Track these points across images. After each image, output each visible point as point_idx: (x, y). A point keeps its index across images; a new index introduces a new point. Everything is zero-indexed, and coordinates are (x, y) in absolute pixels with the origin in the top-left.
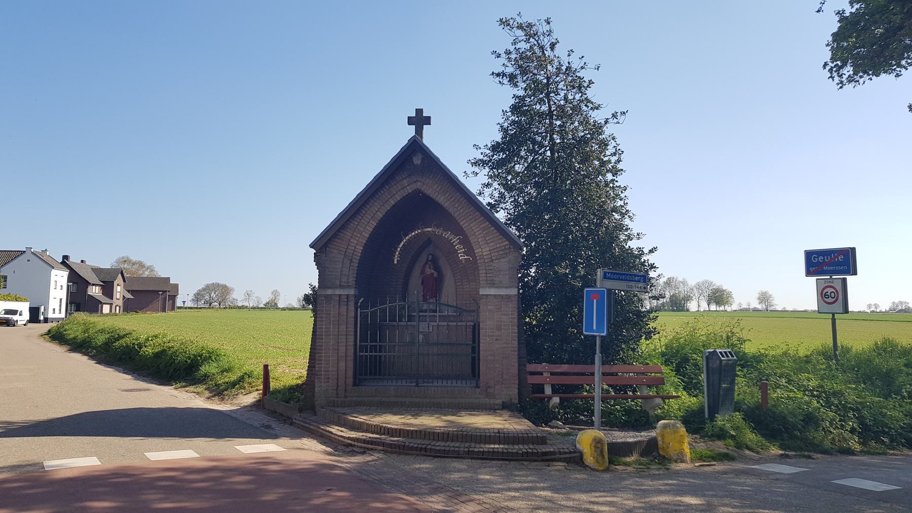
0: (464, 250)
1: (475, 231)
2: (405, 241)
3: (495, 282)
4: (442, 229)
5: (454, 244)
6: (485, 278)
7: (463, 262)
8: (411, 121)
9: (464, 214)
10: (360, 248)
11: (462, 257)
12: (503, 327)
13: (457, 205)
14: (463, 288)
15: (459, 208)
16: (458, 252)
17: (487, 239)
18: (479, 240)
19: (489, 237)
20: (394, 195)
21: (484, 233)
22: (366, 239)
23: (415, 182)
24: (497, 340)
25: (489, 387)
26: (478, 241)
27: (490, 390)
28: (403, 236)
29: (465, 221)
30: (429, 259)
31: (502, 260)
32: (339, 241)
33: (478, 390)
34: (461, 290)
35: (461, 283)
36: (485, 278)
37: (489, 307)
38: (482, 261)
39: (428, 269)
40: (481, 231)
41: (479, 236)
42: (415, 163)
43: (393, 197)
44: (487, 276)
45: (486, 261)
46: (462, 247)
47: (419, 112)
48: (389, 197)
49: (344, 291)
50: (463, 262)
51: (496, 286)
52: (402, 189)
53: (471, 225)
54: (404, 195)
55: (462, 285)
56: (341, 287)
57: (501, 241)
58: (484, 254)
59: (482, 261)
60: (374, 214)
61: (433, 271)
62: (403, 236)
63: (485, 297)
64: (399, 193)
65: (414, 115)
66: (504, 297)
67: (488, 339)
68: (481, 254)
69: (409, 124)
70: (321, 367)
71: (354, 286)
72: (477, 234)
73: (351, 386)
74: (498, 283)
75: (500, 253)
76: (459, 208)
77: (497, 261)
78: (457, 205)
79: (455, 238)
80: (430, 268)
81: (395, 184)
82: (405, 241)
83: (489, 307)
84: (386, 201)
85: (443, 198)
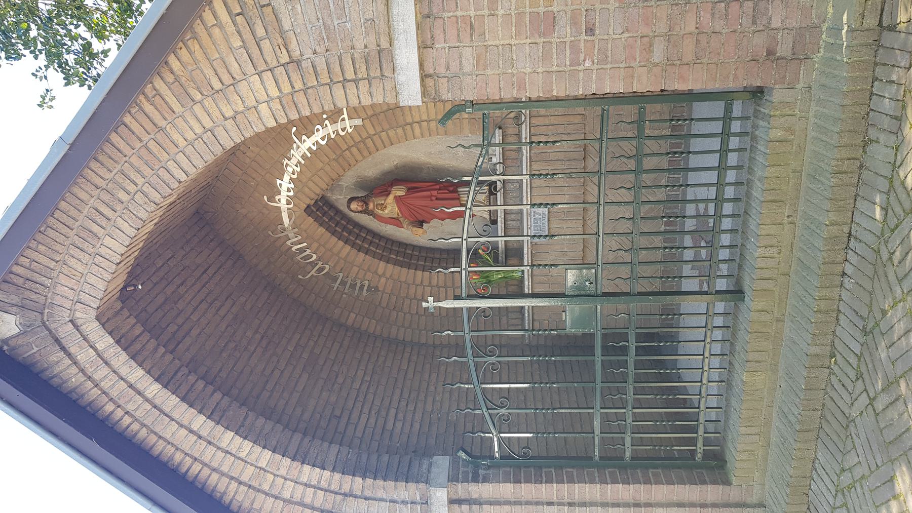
0: (327, 122)
1: (199, 130)
3: (373, 46)
4: (279, 181)
5: (314, 148)
6: (363, 85)
7: (358, 122)
9: (147, 171)
10: (308, 473)
11: (348, 124)
12: (541, 10)
13: (122, 195)
14: (428, 121)
15: (131, 188)
16: (333, 136)
17: (217, 85)
18: (229, 113)
19: (209, 72)
20: (131, 386)
21: (198, 97)
22: (278, 457)
23: (76, 327)
24: (590, 31)
25: (770, 53)
26: (234, 118)
27: (784, 49)
28: (309, 275)
29: (171, 165)
30: (360, 209)
31: (287, 25)
33: (778, 95)
35: (416, 126)
36: (363, 85)
37: (468, 68)
38: (301, 98)
39: (386, 211)
40: (197, 108)
41: (216, 113)
42: (16, 331)
44: (356, 81)
45: (299, 85)
46: (319, 127)
48: (140, 400)
50: (358, 122)
51: (385, 44)
53: (182, 143)
57: (216, 31)
58: (274, 92)
59: (301, 98)
60: (200, 437)
61: (391, 197)
62: (309, 275)
63: (430, 82)
64: (123, 371)
66: (426, 11)
67: (588, 64)
68: (276, 105)
71: (422, 485)
72: (208, 124)
73: (727, 488)
74: (372, 39)
75: (260, 32)
76: (131, 188)
77: (293, 45)
78: (122, 195)
80: (383, 207)
83: (468, 68)
84: (155, 407)
85: (108, 241)
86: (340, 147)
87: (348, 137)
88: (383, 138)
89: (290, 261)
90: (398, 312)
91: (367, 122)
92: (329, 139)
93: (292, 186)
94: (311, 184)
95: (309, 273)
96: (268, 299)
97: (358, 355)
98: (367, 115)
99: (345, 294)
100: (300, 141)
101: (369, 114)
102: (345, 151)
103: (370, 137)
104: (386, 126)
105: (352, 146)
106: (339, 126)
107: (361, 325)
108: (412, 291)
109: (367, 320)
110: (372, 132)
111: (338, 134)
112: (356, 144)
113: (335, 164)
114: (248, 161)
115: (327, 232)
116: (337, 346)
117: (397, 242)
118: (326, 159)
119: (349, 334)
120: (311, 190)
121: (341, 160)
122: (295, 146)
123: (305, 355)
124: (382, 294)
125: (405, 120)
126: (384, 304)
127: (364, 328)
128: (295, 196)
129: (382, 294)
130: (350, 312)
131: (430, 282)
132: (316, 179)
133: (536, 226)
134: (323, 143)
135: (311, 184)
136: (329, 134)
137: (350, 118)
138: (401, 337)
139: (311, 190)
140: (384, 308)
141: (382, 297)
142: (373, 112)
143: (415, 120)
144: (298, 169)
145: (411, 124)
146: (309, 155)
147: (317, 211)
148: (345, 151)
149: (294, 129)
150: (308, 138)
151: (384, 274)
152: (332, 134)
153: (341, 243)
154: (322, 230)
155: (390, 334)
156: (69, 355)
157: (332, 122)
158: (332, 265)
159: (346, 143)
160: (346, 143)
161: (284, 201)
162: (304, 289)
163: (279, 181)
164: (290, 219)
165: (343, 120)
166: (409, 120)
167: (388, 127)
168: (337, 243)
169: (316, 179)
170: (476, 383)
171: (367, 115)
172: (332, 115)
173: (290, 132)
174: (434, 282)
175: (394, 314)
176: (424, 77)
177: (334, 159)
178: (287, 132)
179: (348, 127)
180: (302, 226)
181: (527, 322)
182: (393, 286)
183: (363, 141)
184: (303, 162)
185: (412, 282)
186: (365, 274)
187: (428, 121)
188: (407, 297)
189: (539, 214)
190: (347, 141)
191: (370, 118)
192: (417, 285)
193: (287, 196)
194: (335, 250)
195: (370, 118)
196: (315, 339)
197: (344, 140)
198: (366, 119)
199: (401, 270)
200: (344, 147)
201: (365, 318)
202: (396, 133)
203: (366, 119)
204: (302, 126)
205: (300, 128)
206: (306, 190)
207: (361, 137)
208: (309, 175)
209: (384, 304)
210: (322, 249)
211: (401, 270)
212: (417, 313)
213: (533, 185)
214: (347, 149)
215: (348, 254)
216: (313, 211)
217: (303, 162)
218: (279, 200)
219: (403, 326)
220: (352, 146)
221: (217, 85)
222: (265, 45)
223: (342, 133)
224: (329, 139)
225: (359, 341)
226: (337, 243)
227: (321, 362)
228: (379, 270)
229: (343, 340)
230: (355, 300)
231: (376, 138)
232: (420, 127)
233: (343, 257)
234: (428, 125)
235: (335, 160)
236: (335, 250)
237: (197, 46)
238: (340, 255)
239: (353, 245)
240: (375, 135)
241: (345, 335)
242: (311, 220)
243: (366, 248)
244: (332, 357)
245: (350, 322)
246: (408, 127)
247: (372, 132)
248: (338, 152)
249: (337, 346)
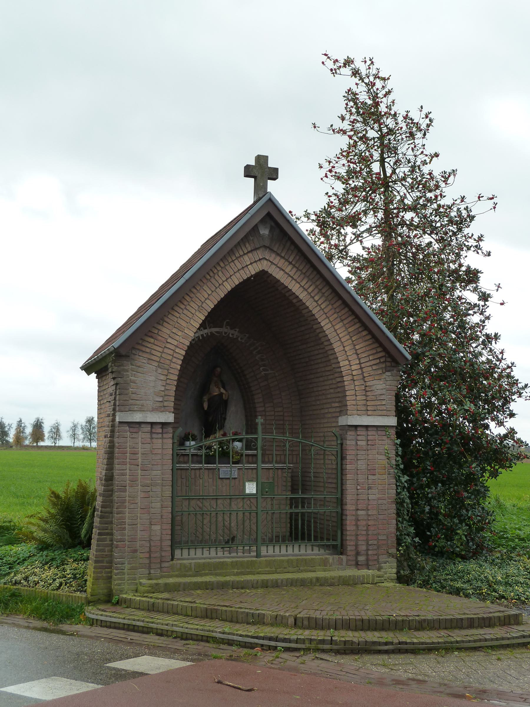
8: (249, 172)
32: (152, 340)
43: (230, 280)
47: (262, 160)
49: (159, 417)
52: (243, 268)
54: (245, 277)
56: (153, 410)
57: (374, 351)
64: (237, 274)
65: (271, 164)
69: (246, 175)
70: (124, 535)
81: (233, 261)
156: (248, 252)
176: (356, 427)
221: (357, 347)
222: (370, 368)
237: (370, 343)
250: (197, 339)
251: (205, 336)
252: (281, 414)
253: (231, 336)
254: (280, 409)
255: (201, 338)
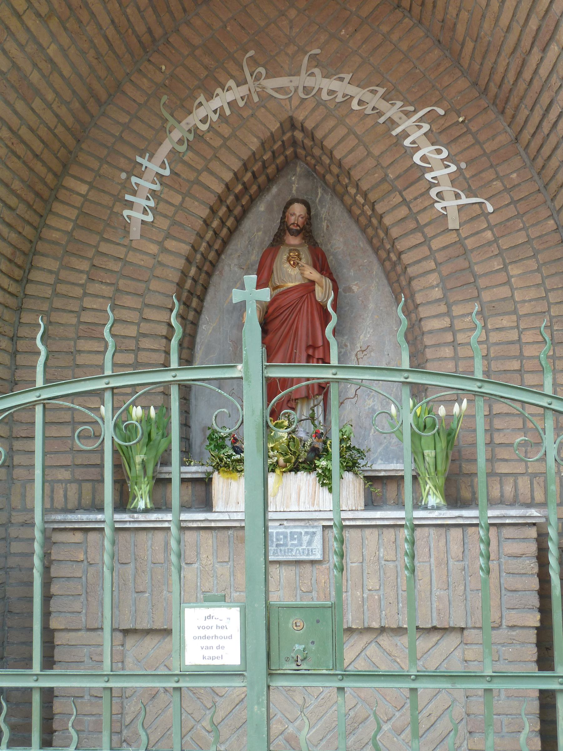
0: (453, 168)
2: (176, 135)
16: (428, 176)
28: (166, 115)
34: (448, 352)
35: (445, 322)
46: (445, 154)
50: (453, 224)
55: (451, 328)
62: (166, 115)
79: (408, 114)
82: (176, 135)
86: (408, 187)
87: (427, 203)
88: (424, 263)
89: (196, 83)
90: (88, 273)
91: (452, 238)
92: (424, 170)
93: (339, 99)
94: (341, 131)
95: (173, 116)
96: (134, 31)
97: (16, 185)
98: (466, 238)
99: (128, 178)
100: (421, 119)
101: (467, 242)
102: (402, 196)
103: (426, 241)
104: (446, 270)
105: (410, 209)
106: (446, 187)
107: (62, 202)
108: (128, 301)
109: (73, 214)
110: (436, 244)
111: (432, 185)
112: (413, 216)
113: (377, 176)
114: (385, 29)
115: (250, 153)
116: (38, 146)
117: (209, 283)
118: (386, 161)
119: (50, 178)
120: (331, 131)
121: (385, 187)
122: (411, 108)
123: (35, 77)
124: (125, 246)
125: (456, 303)
126: (104, 248)
127: (58, 207)
128: (320, 103)
129: (125, 246)
130: (90, 184)
131: (145, 335)
132: (352, 142)
133: (285, 537)
134: (417, 158)
135: (341, 131)
136: (431, 170)
137: (461, 208)
138: (35, 275)
139: (331, 131)
140: (97, 247)
141: (118, 244)
142: (469, 248)
143: (456, 322)
144: (369, 111)
145: (448, 313)
146: (394, 133)
147: (283, 142)
148: (402, 196)
149: (442, 112)
150: (425, 134)
151: (165, 250)
152: (433, 174)
153: (228, 176)
154: (254, 144)
155: (43, 255)
157: (453, 177)
158: (185, 158)
159: (416, 199)
160: (416, 199)
161: (310, 82)
162: (139, 105)
163: (348, 77)
164: (277, 90)
165: (457, 196)
166: (457, 310)
167: (445, 273)
168: (229, 169)
169: (352, 142)
170: (46, 394)
171: (466, 238)
172: (465, 178)
173: (436, 104)
174: (146, 343)
175: (85, 266)
177: (386, 175)
178: (434, 100)
179: (444, 204)
180: (263, 110)
181: (85, 517)
182: (140, 266)
183: (419, 228)
184: (382, 120)
185: (147, 301)
186: (165, 216)
187: (454, 344)
188: (118, 290)
189: (310, 543)
190: (419, 200)
191: (460, 242)
192: (140, 311)
193: (320, 90)
194: (215, 166)
195: (460, 242)
196: (54, 106)
197: (422, 195)
198: (459, 235)
199: (172, 282)
200: (409, 195)
201: (76, 212)
202: (433, 287)
203: (459, 235)
204: (447, 125)
205: (442, 121)
206: (331, 123)
207: (426, 225)
208: (359, 130)
209: (104, 248)
210: (217, 142)
211: (172, 282)
212: (84, 309)
213: (367, 531)
214: (404, 200)
215: (208, 188)
216: (284, 133)
217: (382, 120)
218: (312, 74)
219: (59, 281)
220: (410, 209)
223: (433, 193)
224: (424, 170)
225: (37, 194)
226: (229, 169)
227: (20, 106)
228: (174, 243)
229: (44, 164)
230: (113, 195)
231: (424, 251)
232: (444, 330)
233: (200, 178)
234: (446, 344)
235: (384, 179)
236: (215, 166)
238: (205, 174)
239: (221, 200)
240: (430, 249)
241: (50, 170)
242: (274, 126)
243: (212, 222)
244: (24, 132)
245: (70, 182)
246: (443, 308)
247: (436, 244)
248: (399, 184)
249: (38, 146)
250: (215, 117)
251: (241, 104)
252: (513, 335)
253: (325, 96)
254: (506, 321)
255: (228, 112)
